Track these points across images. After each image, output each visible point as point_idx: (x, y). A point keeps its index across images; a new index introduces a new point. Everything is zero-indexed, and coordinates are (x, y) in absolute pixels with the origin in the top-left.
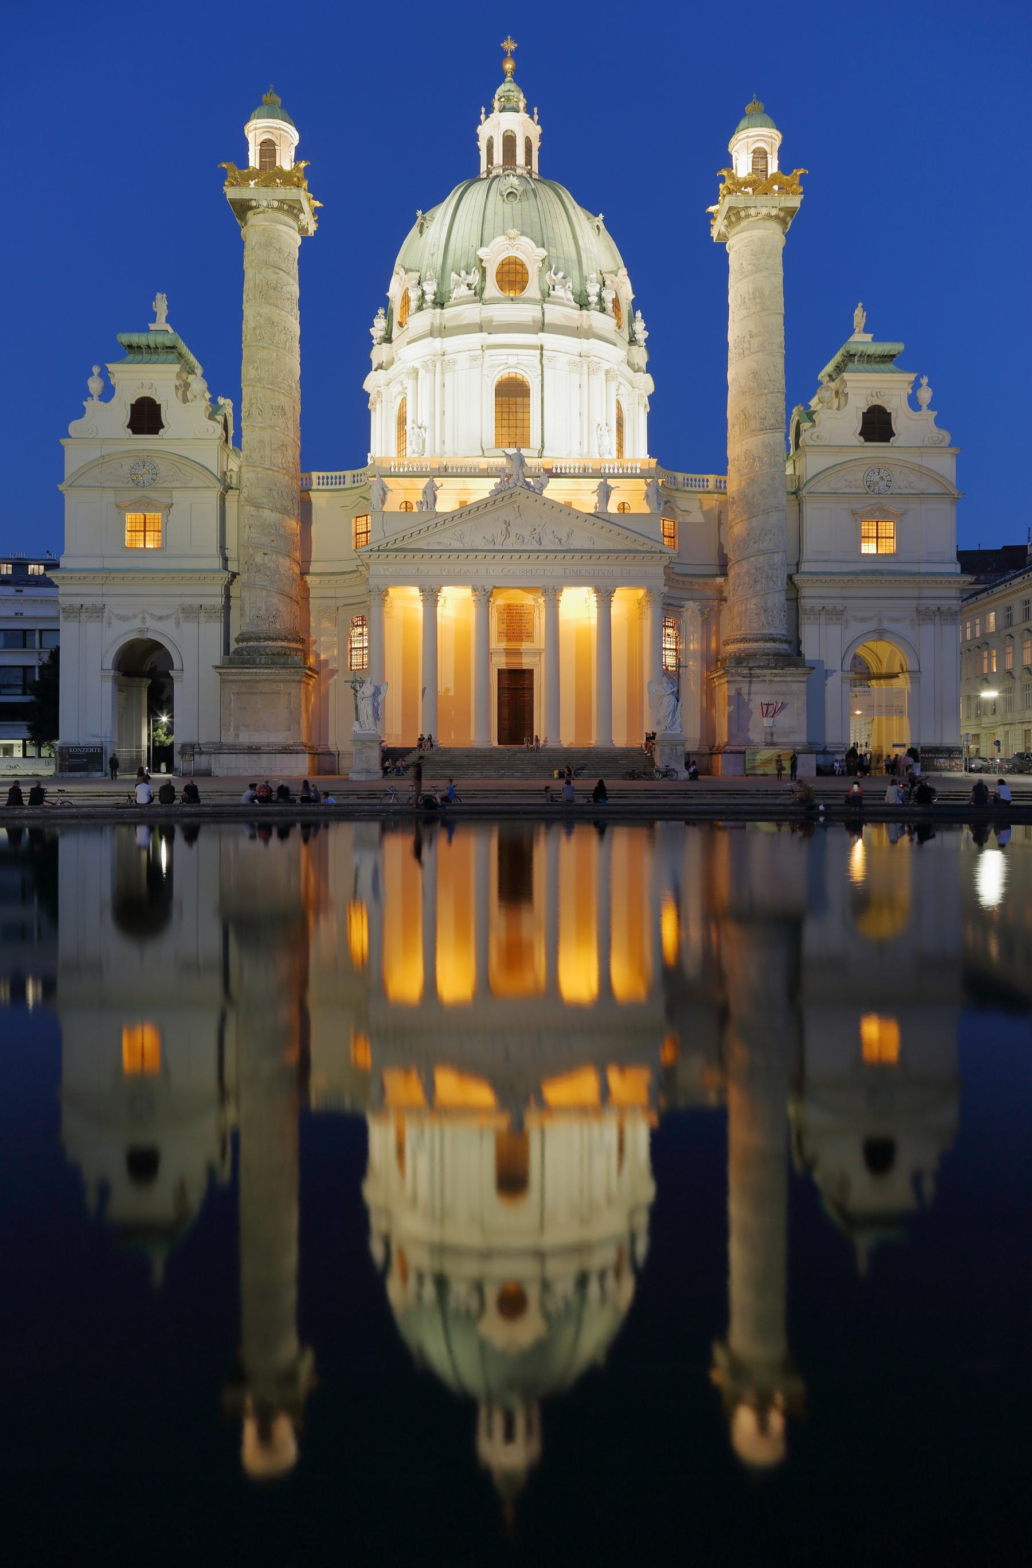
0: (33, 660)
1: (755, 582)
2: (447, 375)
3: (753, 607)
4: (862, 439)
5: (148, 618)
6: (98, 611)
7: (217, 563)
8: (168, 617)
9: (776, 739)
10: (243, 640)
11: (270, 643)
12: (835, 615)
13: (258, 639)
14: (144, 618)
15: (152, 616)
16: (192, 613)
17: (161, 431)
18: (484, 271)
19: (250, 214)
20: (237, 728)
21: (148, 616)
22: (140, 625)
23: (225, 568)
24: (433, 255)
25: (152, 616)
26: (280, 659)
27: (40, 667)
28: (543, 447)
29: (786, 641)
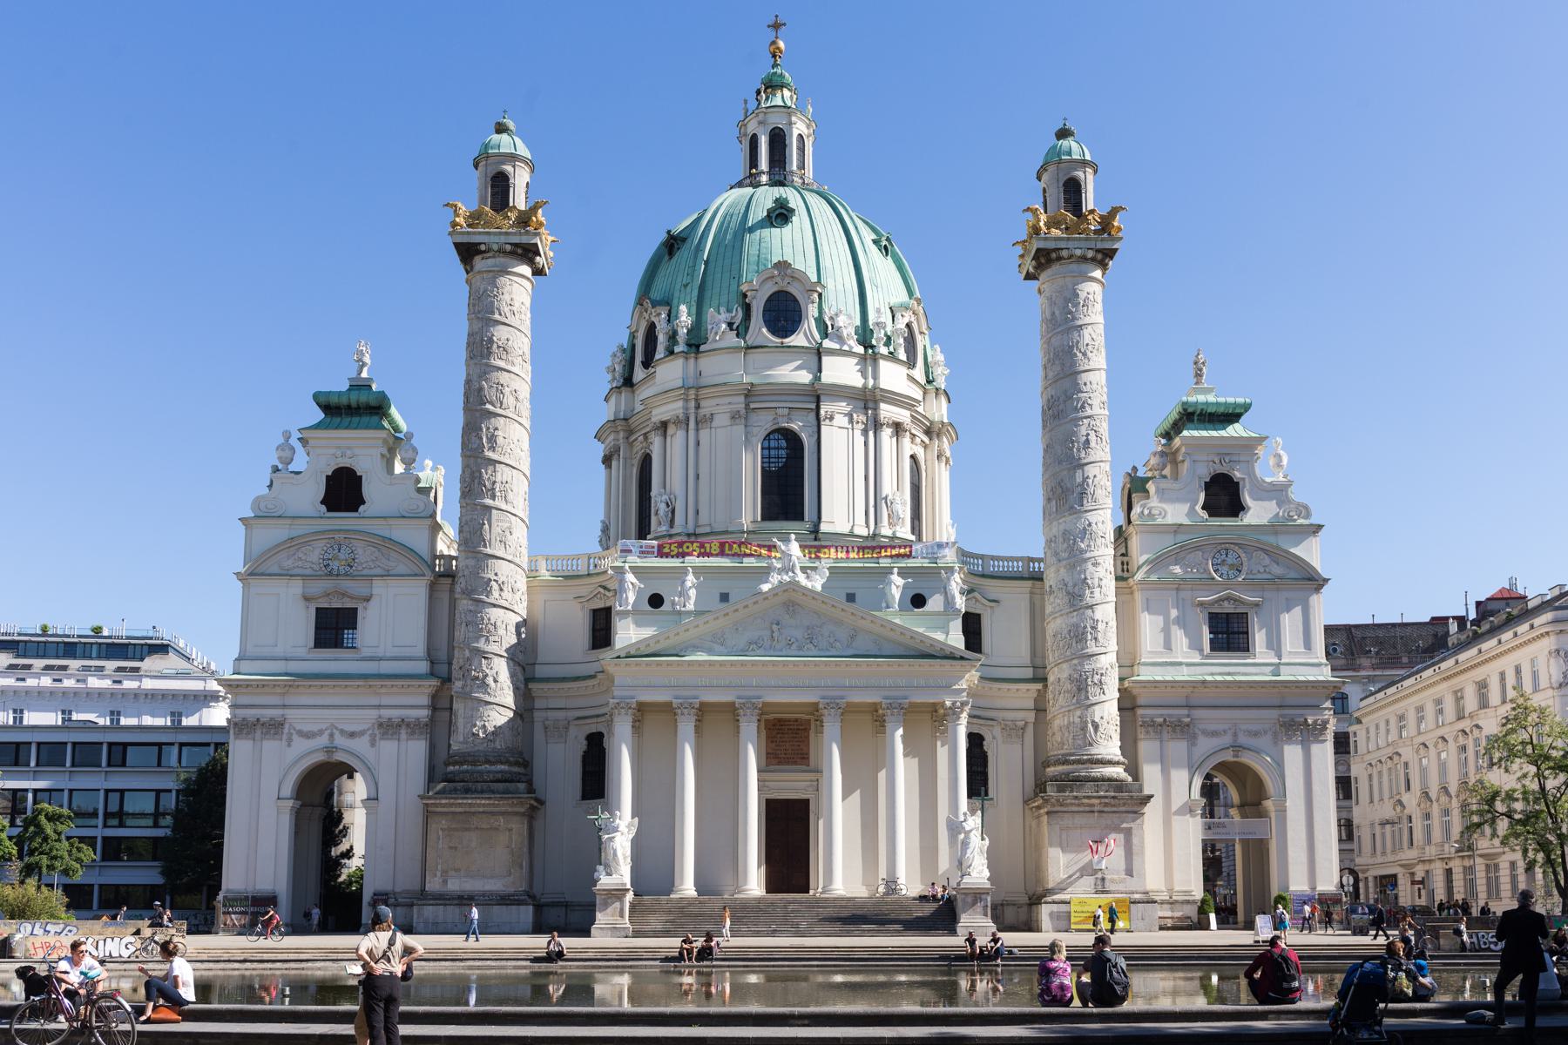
0: (170, 783)
1: (1079, 690)
2: (702, 433)
3: (1077, 720)
5: (337, 733)
6: (274, 727)
7: (423, 667)
8: (362, 733)
10: (455, 763)
12: (1182, 729)
13: (474, 763)
14: (331, 735)
16: (388, 728)
17: (362, 508)
18: (747, 309)
19: (477, 259)
20: (444, 872)
21: (337, 733)
23: (432, 674)
24: (686, 286)
25: (342, 732)
27: (178, 791)
28: (819, 518)
29: (1118, 763)
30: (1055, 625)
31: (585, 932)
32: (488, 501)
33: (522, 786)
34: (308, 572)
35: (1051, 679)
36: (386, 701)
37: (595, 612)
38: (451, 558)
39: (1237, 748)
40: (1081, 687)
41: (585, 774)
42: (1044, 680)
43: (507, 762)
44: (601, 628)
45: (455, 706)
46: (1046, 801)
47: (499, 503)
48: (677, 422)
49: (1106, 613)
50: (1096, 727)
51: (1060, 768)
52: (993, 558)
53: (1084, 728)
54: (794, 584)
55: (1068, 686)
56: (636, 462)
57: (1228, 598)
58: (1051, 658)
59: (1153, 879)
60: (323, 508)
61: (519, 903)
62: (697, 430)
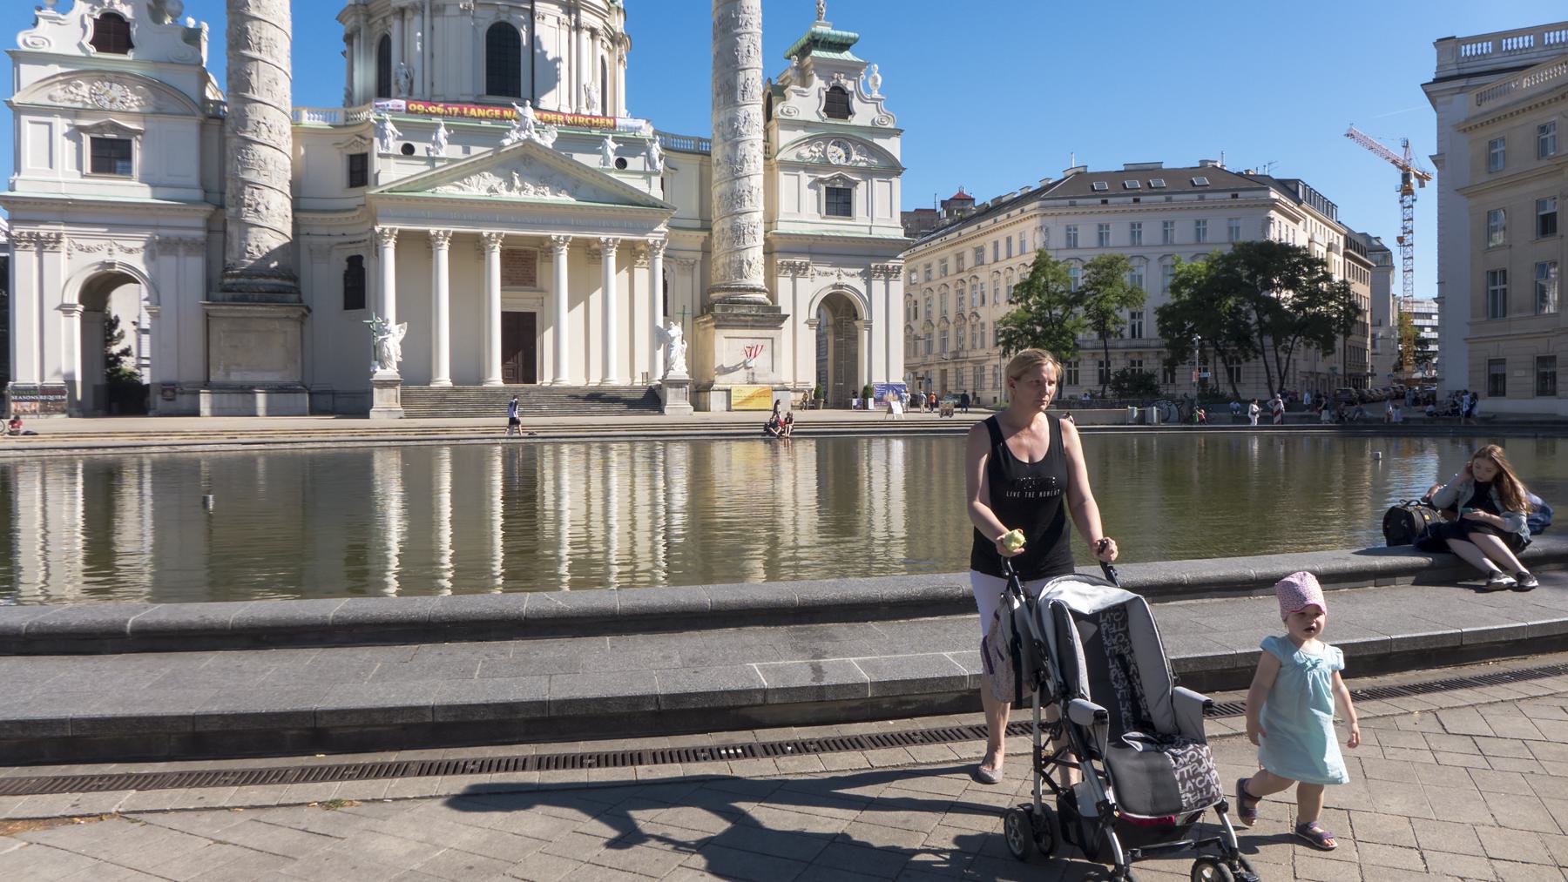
4: (824, 115)
7: (197, 194)
9: (757, 378)
11: (262, 280)
15: (121, 248)
22: (108, 259)
25: (121, 248)
26: (272, 296)
30: (717, 190)
31: (366, 415)
32: (255, 54)
33: (294, 297)
34: (79, 105)
35: (716, 228)
36: (163, 222)
37: (352, 158)
38: (220, 103)
39: (841, 287)
40: (737, 234)
41: (347, 290)
42: (710, 229)
43: (283, 278)
44: (359, 170)
45: (230, 228)
46: (714, 317)
47: (263, 56)
48: (414, 9)
49: (757, 181)
50: (750, 265)
51: (722, 294)
52: (673, 136)
53: (741, 268)
54: (529, 141)
55: (730, 234)
56: (376, 41)
57: (841, 177)
58: (716, 212)
59: (786, 377)
60: (92, 50)
61: (296, 391)
62: (432, 17)
